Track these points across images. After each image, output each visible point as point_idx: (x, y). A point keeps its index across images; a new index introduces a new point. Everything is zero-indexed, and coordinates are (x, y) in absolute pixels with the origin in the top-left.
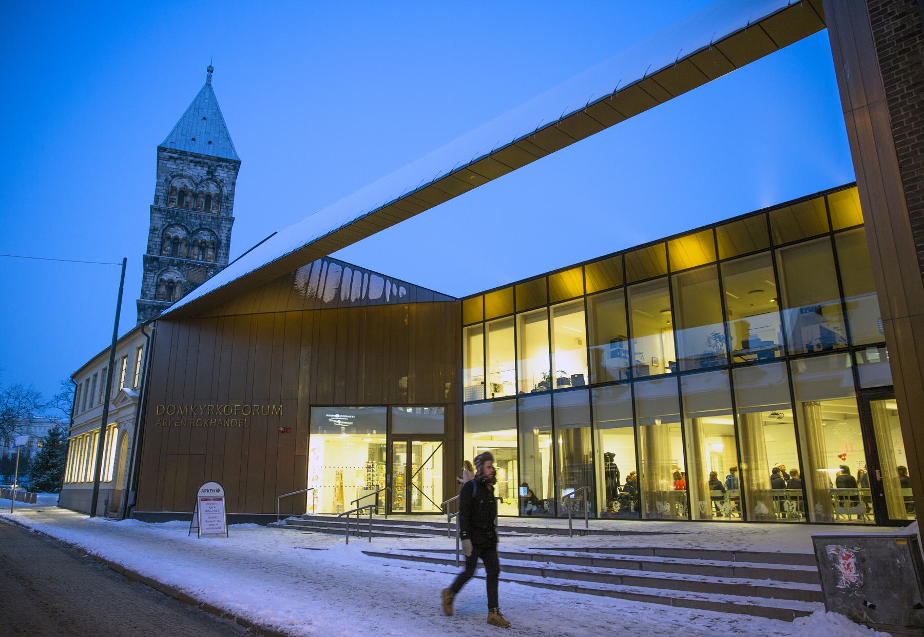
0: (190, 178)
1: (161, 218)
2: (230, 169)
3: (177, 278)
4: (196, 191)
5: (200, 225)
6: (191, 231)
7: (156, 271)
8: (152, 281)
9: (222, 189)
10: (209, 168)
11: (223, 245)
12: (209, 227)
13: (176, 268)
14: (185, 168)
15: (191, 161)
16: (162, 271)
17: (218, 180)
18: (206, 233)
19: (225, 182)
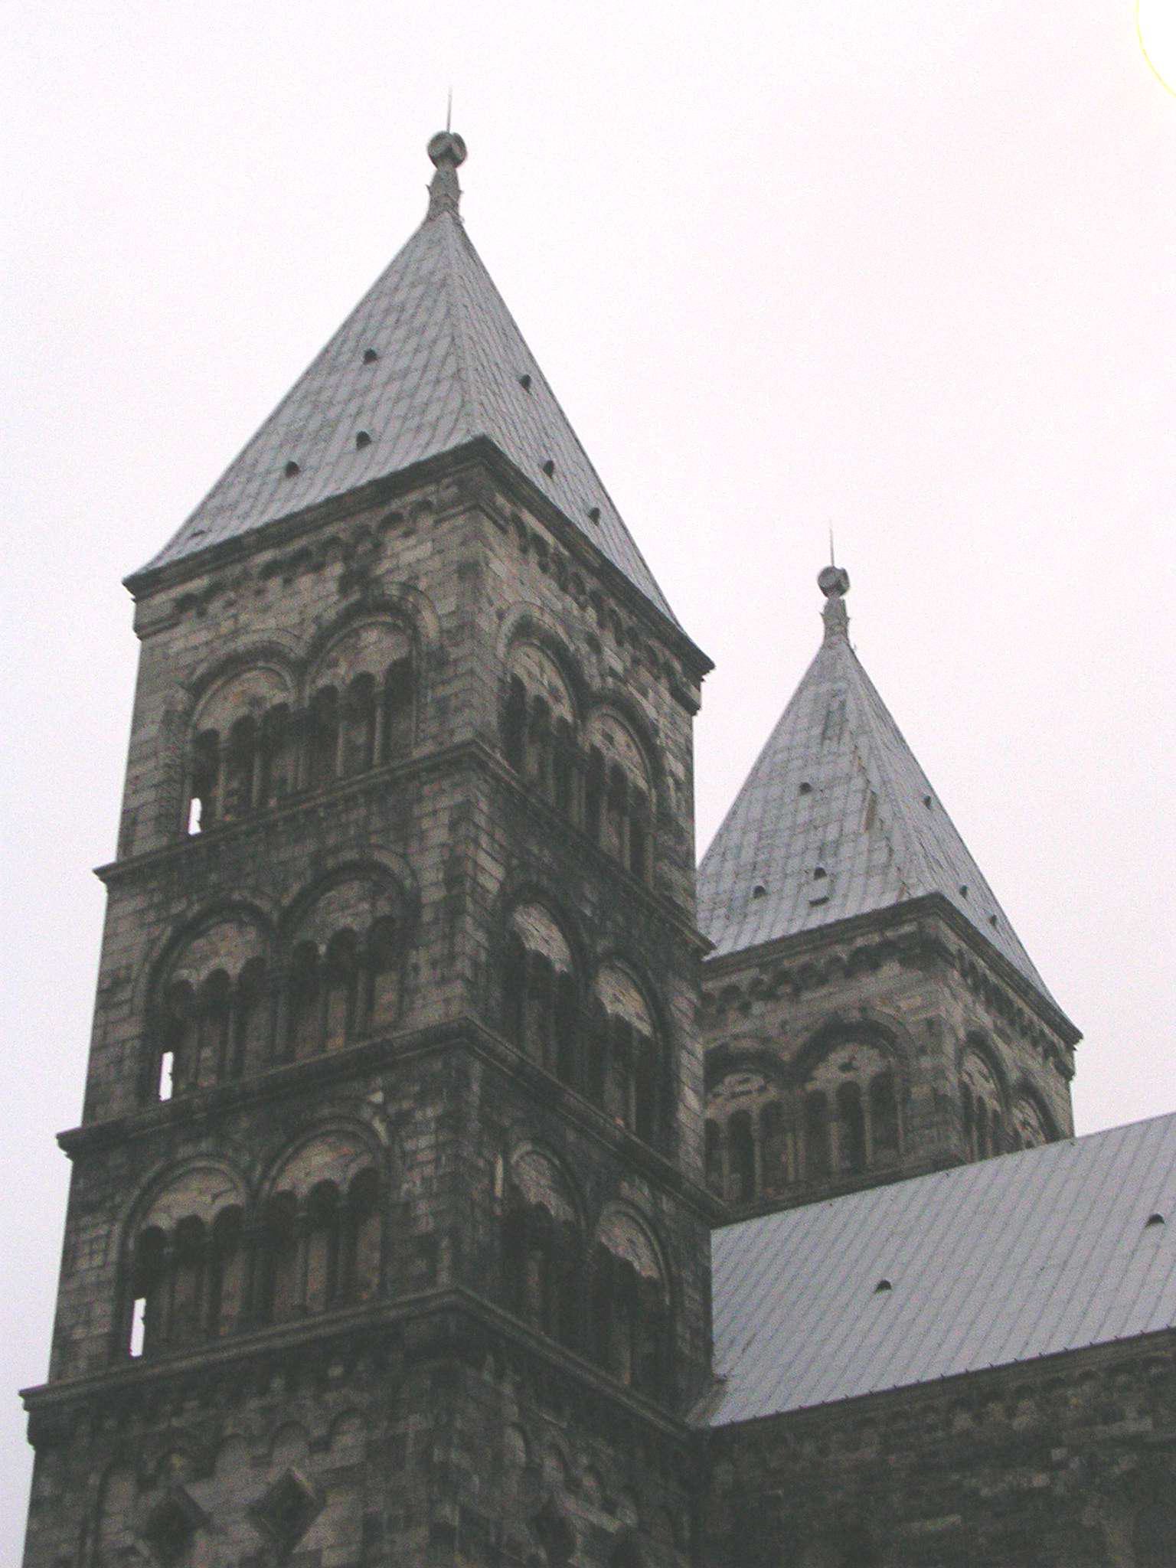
0: (269, 653)
1: (142, 912)
2: (443, 507)
3: (215, 1197)
4: (299, 700)
5: (317, 859)
6: (275, 917)
7: (118, 1199)
8: (98, 1260)
9: (415, 629)
10: (346, 559)
11: (427, 916)
12: (351, 855)
13: (205, 1146)
14: (243, 618)
15: (269, 571)
16: (147, 1189)
17: (394, 591)
18: (351, 891)
19: (422, 585)
